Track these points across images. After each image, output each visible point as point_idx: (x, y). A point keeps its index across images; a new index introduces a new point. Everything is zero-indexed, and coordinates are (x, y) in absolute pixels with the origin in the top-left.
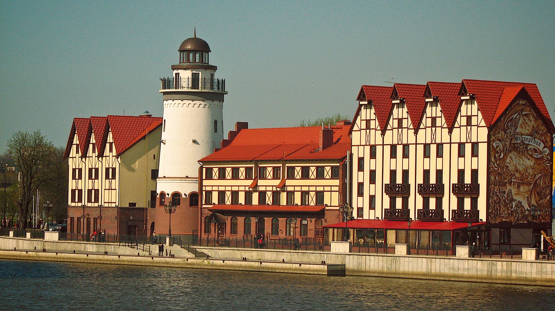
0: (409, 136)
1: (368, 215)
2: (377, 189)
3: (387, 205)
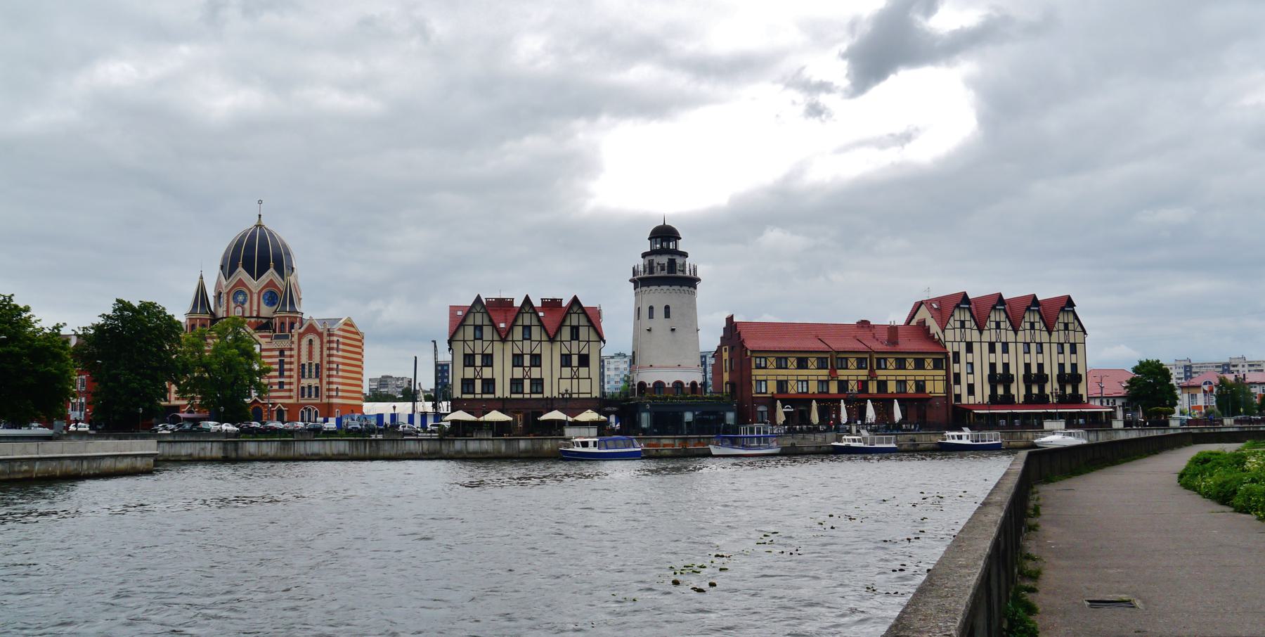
1: (965, 400)
3: (987, 391)
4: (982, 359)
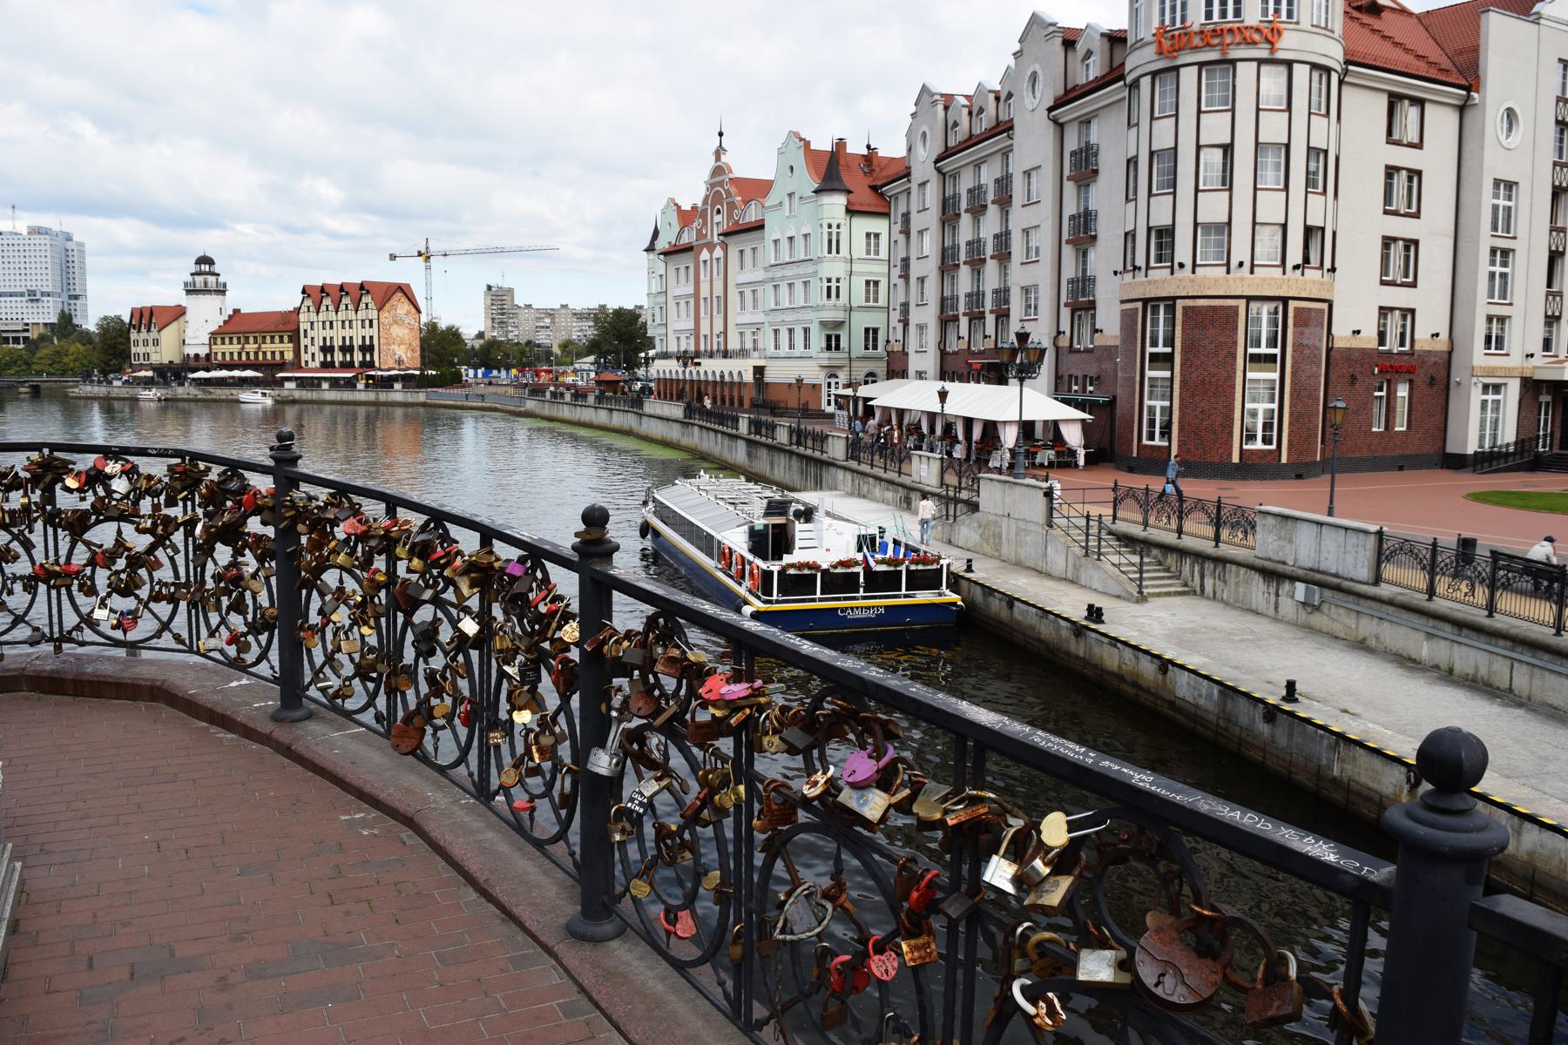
0: (332, 316)
2: (315, 349)
4: (319, 334)
